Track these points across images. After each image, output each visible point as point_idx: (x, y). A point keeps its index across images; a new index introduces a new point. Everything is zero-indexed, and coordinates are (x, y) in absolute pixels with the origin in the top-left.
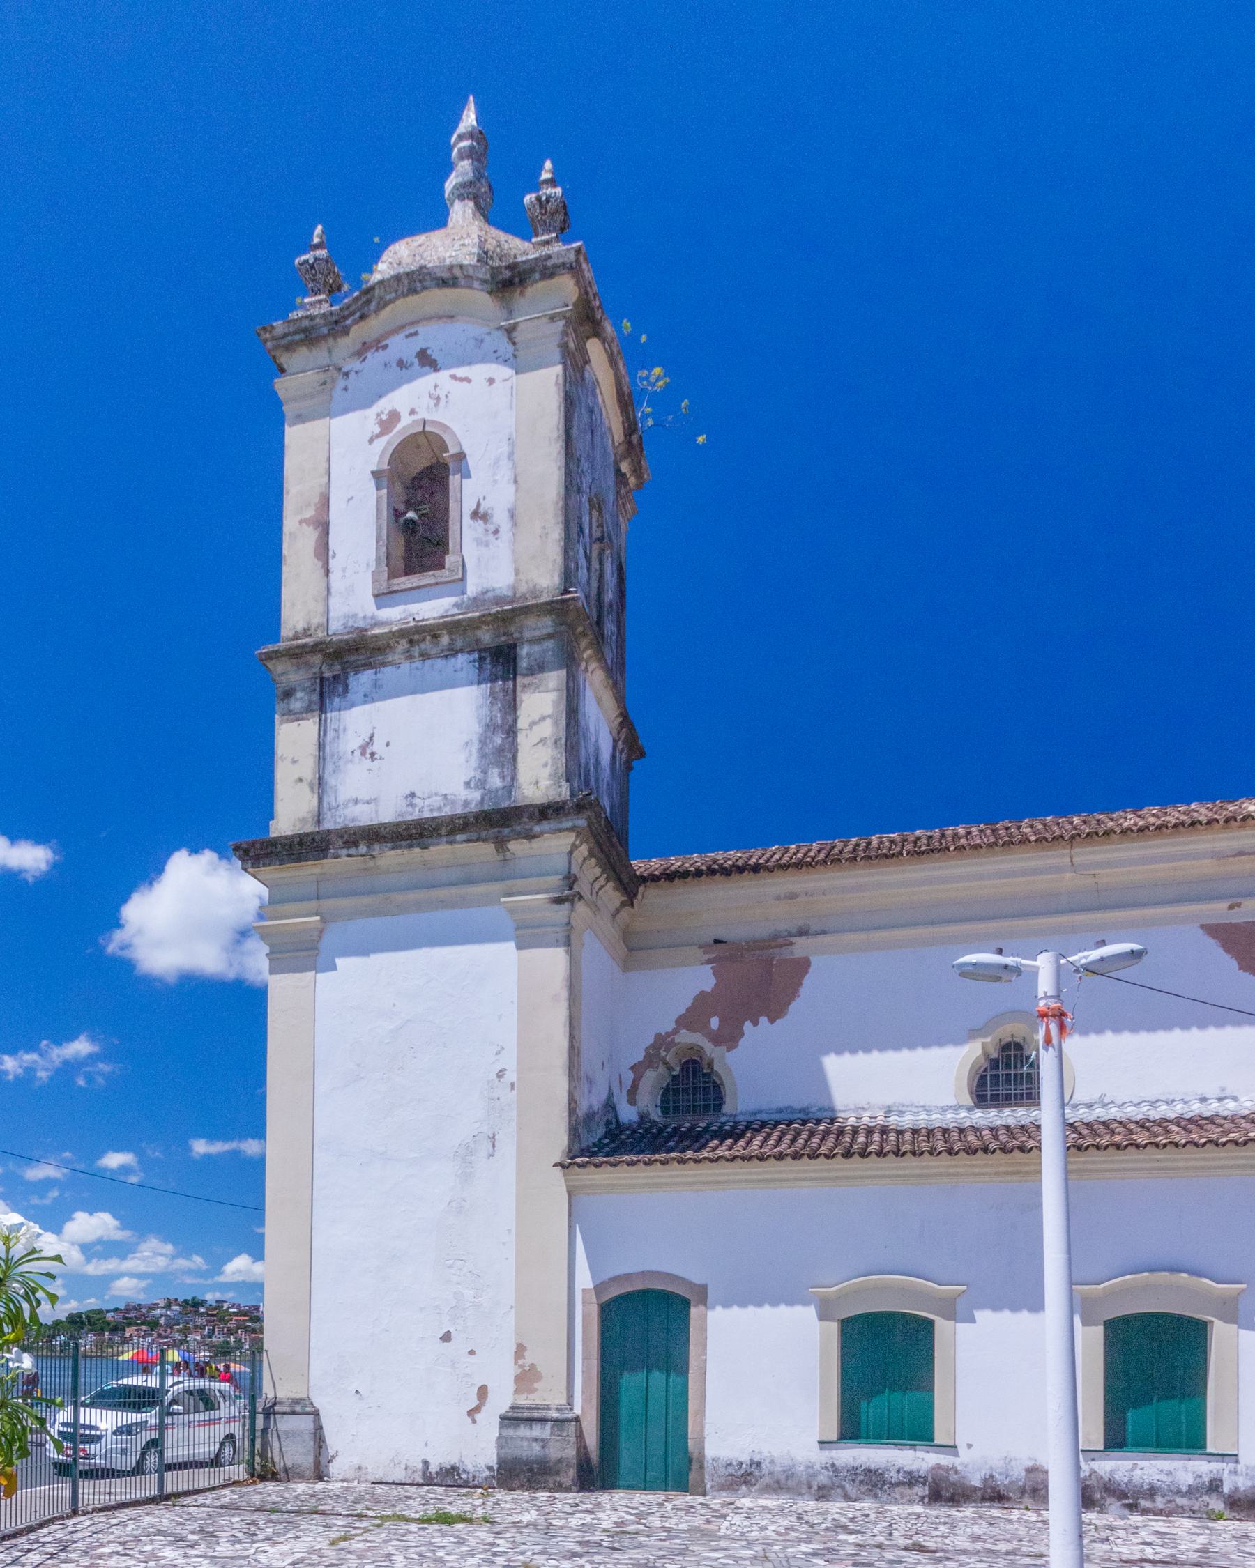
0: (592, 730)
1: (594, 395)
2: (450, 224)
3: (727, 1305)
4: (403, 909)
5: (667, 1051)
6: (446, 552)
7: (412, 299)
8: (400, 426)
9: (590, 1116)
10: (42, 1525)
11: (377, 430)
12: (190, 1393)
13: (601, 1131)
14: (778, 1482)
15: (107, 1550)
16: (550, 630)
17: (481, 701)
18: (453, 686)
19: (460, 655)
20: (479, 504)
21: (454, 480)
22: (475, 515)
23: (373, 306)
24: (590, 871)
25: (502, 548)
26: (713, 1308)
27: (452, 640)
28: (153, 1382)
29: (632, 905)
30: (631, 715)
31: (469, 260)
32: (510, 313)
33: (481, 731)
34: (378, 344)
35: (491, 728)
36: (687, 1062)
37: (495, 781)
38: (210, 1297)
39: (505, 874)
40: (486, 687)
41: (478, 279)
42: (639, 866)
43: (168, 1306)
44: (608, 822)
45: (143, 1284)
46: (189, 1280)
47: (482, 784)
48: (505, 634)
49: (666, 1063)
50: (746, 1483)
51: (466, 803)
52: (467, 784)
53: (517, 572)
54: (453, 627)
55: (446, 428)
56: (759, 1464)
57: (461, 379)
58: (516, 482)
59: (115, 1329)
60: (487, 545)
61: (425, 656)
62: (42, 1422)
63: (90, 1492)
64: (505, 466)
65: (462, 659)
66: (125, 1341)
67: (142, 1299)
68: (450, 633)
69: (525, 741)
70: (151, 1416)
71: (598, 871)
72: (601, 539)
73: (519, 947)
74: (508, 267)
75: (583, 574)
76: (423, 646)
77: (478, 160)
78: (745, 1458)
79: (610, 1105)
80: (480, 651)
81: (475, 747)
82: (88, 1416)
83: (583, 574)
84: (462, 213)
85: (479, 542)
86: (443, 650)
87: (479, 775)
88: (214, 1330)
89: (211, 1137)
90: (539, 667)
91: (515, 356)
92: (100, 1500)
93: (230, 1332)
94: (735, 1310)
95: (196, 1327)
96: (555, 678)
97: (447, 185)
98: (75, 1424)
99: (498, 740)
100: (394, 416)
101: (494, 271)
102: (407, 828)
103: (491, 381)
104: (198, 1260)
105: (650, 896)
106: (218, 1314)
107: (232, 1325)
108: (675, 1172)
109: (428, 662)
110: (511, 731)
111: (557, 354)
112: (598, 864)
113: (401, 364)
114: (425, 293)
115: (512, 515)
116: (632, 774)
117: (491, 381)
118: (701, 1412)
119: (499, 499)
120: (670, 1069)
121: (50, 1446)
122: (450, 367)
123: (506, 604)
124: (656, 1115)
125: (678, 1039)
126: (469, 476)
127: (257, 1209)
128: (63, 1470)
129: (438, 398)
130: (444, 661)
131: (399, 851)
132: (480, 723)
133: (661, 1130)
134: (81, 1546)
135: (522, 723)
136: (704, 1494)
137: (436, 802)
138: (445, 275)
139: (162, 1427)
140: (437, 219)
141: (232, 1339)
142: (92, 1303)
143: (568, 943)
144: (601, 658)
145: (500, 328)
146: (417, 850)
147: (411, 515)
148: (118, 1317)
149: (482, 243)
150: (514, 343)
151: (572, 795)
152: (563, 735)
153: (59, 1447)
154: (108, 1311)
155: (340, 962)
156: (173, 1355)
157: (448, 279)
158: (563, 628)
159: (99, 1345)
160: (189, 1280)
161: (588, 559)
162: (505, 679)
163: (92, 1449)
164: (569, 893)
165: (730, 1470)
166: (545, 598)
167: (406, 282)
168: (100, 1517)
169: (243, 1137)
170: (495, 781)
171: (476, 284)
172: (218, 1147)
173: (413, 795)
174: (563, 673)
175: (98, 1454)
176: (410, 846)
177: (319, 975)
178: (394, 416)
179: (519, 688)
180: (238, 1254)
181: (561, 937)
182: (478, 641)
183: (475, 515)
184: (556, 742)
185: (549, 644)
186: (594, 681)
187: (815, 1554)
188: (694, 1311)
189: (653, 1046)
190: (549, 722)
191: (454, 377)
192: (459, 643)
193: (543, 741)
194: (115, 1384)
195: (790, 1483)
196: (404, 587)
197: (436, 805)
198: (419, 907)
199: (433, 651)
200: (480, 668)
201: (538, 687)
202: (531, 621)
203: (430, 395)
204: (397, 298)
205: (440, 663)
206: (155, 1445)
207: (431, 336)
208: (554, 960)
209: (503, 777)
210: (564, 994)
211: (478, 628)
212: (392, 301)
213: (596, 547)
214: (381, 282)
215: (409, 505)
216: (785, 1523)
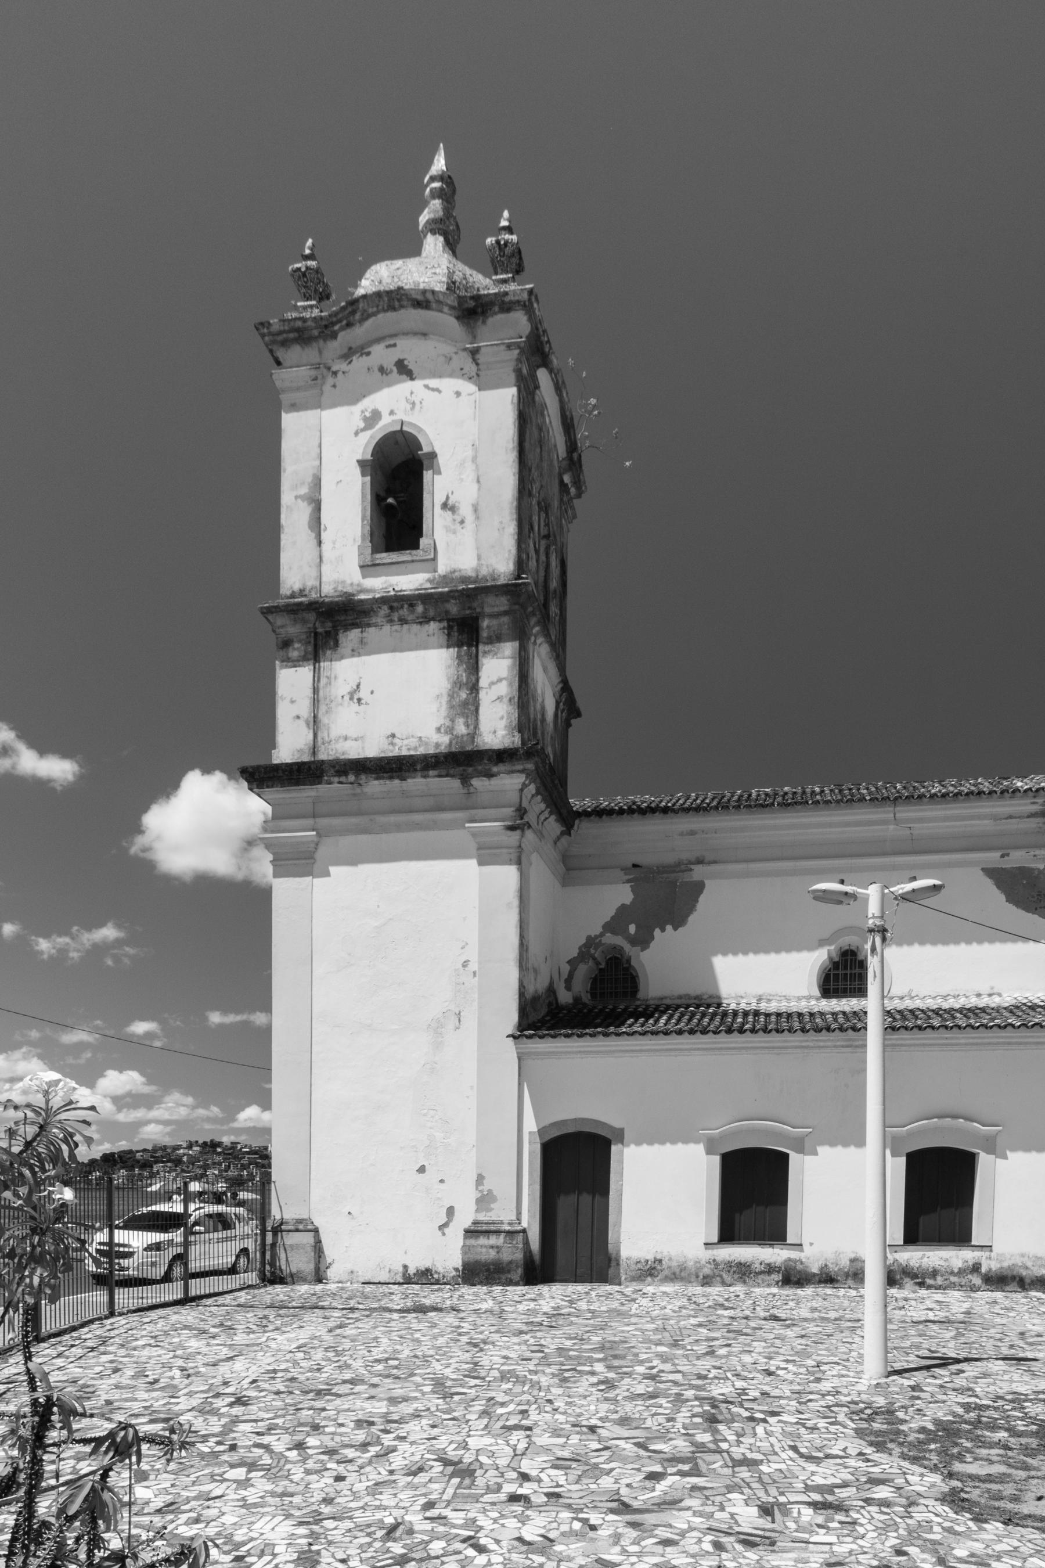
0: (539, 691)
1: (543, 415)
2: (424, 254)
3: (638, 1143)
4: (385, 829)
5: (596, 949)
6: (421, 535)
7: (390, 315)
8: (381, 424)
9: (535, 999)
10: (83, 1325)
11: (362, 425)
12: (210, 1216)
13: (544, 1011)
14: (674, 1274)
15: (140, 1343)
16: (506, 608)
17: (450, 662)
18: (426, 648)
19: (432, 623)
20: (448, 498)
21: (427, 475)
22: (445, 506)
23: (358, 316)
24: (537, 807)
25: (467, 536)
26: (628, 1146)
27: (425, 609)
28: (178, 1208)
29: (570, 835)
30: (572, 683)
31: (440, 288)
32: (474, 338)
33: (449, 686)
34: (362, 350)
35: (457, 684)
36: (610, 959)
37: (461, 729)
38: (226, 1140)
39: (469, 804)
40: (453, 651)
41: (447, 305)
42: (575, 803)
43: (190, 1146)
44: (551, 768)
45: (168, 1129)
46: (207, 1126)
47: (450, 730)
48: (470, 608)
49: (594, 959)
50: (651, 1275)
51: (437, 745)
52: (438, 730)
53: (479, 558)
54: (425, 598)
55: (420, 430)
56: (660, 1261)
57: (433, 390)
58: (478, 481)
59: (146, 1165)
60: (455, 533)
61: (403, 621)
62: (83, 1242)
63: (124, 1297)
64: (470, 467)
65: (433, 626)
66: (152, 1175)
67: (168, 1141)
68: (424, 603)
69: (486, 697)
70: (177, 1236)
71: (543, 806)
72: (547, 537)
73: (481, 863)
74: (472, 298)
75: (532, 564)
76: (401, 612)
77: (448, 202)
78: (650, 1257)
79: (551, 990)
80: (449, 620)
81: (445, 699)
82: (121, 1236)
83: (532, 564)
84: (434, 244)
85: (447, 529)
86: (418, 618)
87: (448, 723)
88: (229, 1166)
89: (225, 1011)
90: (497, 638)
91: (478, 375)
92: (134, 1303)
93: (244, 1167)
94: (645, 1148)
95: (214, 1163)
96: (509, 648)
97: (421, 219)
98: (111, 1243)
99: (464, 695)
100: (376, 415)
101: (461, 299)
102: (388, 763)
103: (458, 394)
104: (215, 1110)
105: (583, 827)
106: (233, 1153)
107: (245, 1161)
108: (600, 1044)
109: (405, 627)
110: (474, 688)
111: (512, 377)
112: (544, 800)
113: (382, 370)
114: (402, 311)
115: (476, 509)
116: (570, 730)
117: (458, 394)
118: (619, 1224)
119: (465, 495)
120: (598, 963)
121: (89, 1261)
122: (423, 378)
123: (471, 583)
124: (586, 998)
125: (604, 940)
126: (440, 473)
127: (265, 1069)
128: (101, 1280)
129: (414, 404)
130: (419, 627)
131: (382, 781)
132: (448, 680)
133: (590, 1011)
134: (118, 1340)
135: (483, 682)
136: (620, 1284)
137: (413, 742)
138: (420, 297)
139: (186, 1244)
140: (413, 249)
141: (245, 1173)
142: (123, 1145)
143: (519, 862)
144: (547, 635)
145: (465, 349)
146: (397, 782)
147: (390, 500)
148: (147, 1156)
149: (450, 274)
150: (477, 364)
151: (523, 742)
152: (516, 694)
153: (96, 1261)
154: (138, 1151)
155: (333, 869)
156: (195, 1187)
157: (422, 301)
158: (517, 607)
159: (130, 1178)
160: (207, 1126)
161: (537, 551)
162: (469, 645)
163: (125, 1262)
164: (519, 824)
165: (639, 1266)
166: (502, 581)
167: (386, 299)
168: (135, 1317)
169: (253, 1010)
170: (461, 729)
171: (446, 309)
172: (231, 1018)
173: (393, 736)
174: (516, 644)
175: (131, 1267)
176: (391, 778)
177: (315, 880)
178: (376, 415)
179: (480, 654)
180: (249, 1105)
181: (514, 857)
182: (447, 612)
183: (445, 506)
184: (510, 700)
185: (505, 619)
186: (541, 654)
187: (700, 1325)
188: (614, 1148)
189: (585, 945)
190: (504, 683)
191: (427, 387)
192: (431, 613)
193: (500, 698)
194: (145, 1210)
195: (683, 1274)
196: (385, 561)
197: (413, 745)
198: (399, 828)
199: (410, 618)
200: (449, 635)
201: (496, 654)
202: (490, 600)
203: (407, 400)
204: (378, 312)
205: (415, 628)
206: (181, 1258)
207: (409, 349)
208: (508, 876)
209: (467, 726)
210: (516, 903)
211: (448, 601)
212: (374, 314)
213: (543, 542)
214: (364, 297)
215: (389, 492)
216: (679, 1303)
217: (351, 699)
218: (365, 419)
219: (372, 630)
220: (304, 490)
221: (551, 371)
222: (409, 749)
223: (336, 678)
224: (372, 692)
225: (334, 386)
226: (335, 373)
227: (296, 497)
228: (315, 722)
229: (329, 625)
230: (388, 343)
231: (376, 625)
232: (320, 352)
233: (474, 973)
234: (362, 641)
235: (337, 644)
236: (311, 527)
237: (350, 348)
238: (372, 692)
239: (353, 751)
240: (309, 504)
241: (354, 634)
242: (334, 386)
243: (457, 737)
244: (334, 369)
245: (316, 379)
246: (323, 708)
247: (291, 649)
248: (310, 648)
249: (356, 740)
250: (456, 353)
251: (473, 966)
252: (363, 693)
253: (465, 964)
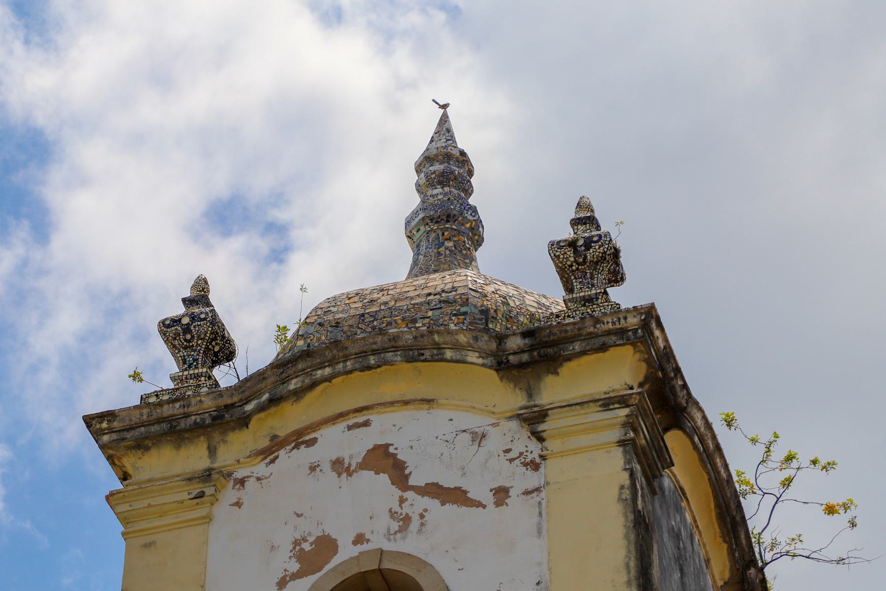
11: (294, 566)
55: (422, 564)
129: (407, 519)
203: (392, 514)
218: (301, 556)
221: (691, 433)
225: (238, 504)
226: (242, 482)
230: (351, 422)
232: (212, 452)
242: (238, 504)
244: (239, 475)
245: (201, 495)
250: (495, 425)
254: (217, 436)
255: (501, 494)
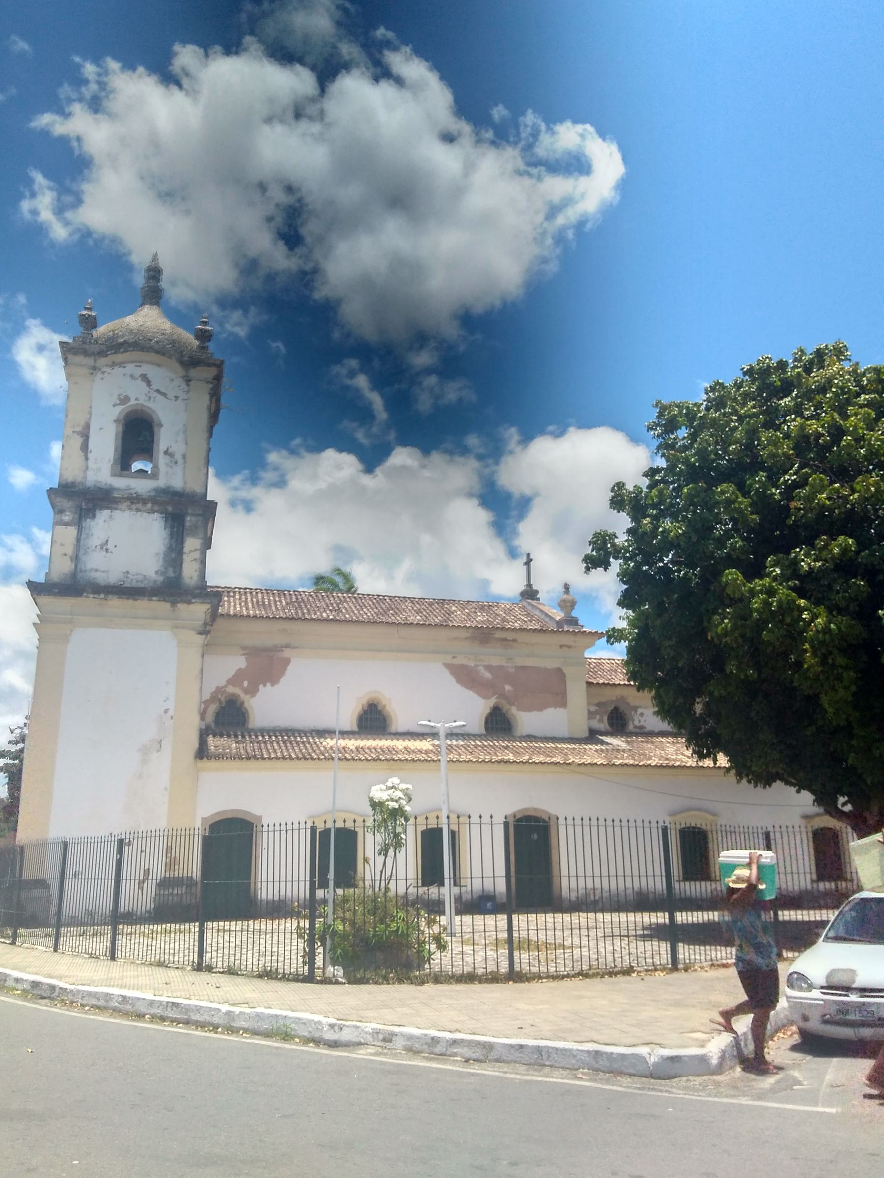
19: (156, 514)
20: (168, 449)
34: (121, 364)
37: (171, 573)
47: (163, 573)
51: (155, 581)
52: (157, 572)
53: (185, 483)
60: (171, 467)
61: (138, 510)
80: (166, 514)
81: (161, 556)
85: (167, 465)
109: (139, 513)
115: (184, 457)
129: (150, 397)
137: (140, 577)
173: (128, 572)
183: (166, 452)
193: (195, 560)
199: (143, 509)
200: (166, 521)
203: (146, 395)
205: (145, 514)
209: (175, 572)
217: (102, 548)
218: (120, 399)
219: (118, 512)
220: (79, 429)
222: (137, 582)
223: (92, 535)
224: (116, 546)
225: (102, 379)
226: (104, 372)
227: (73, 432)
228: (76, 558)
229: (90, 505)
231: (120, 510)
232: (95, 361)
233: (172, 718)
234: (111, 516)
235: (94, 517)
236: (81, 449)
237: (114, 362)
238: (116, 546)
239: (100, 578)
240: (82, 437)
241: (106, 513)
243: (168, 577)
246: (82, 552)
247: (63, 515)
248: (76, 516)
249: (103, 572)
251: (171, 713)
252: (110, 546)
253: (166, 711)
254: (97, 357)
255: (177, 398)
